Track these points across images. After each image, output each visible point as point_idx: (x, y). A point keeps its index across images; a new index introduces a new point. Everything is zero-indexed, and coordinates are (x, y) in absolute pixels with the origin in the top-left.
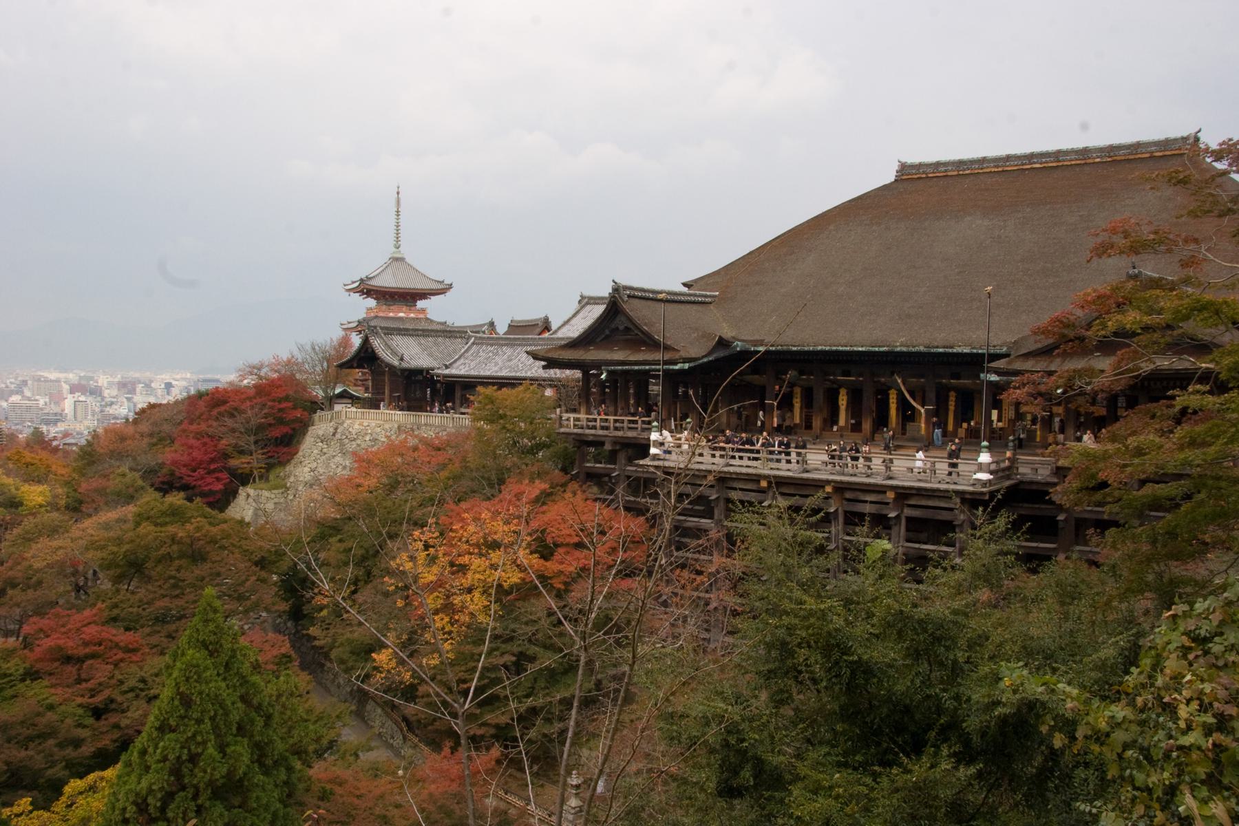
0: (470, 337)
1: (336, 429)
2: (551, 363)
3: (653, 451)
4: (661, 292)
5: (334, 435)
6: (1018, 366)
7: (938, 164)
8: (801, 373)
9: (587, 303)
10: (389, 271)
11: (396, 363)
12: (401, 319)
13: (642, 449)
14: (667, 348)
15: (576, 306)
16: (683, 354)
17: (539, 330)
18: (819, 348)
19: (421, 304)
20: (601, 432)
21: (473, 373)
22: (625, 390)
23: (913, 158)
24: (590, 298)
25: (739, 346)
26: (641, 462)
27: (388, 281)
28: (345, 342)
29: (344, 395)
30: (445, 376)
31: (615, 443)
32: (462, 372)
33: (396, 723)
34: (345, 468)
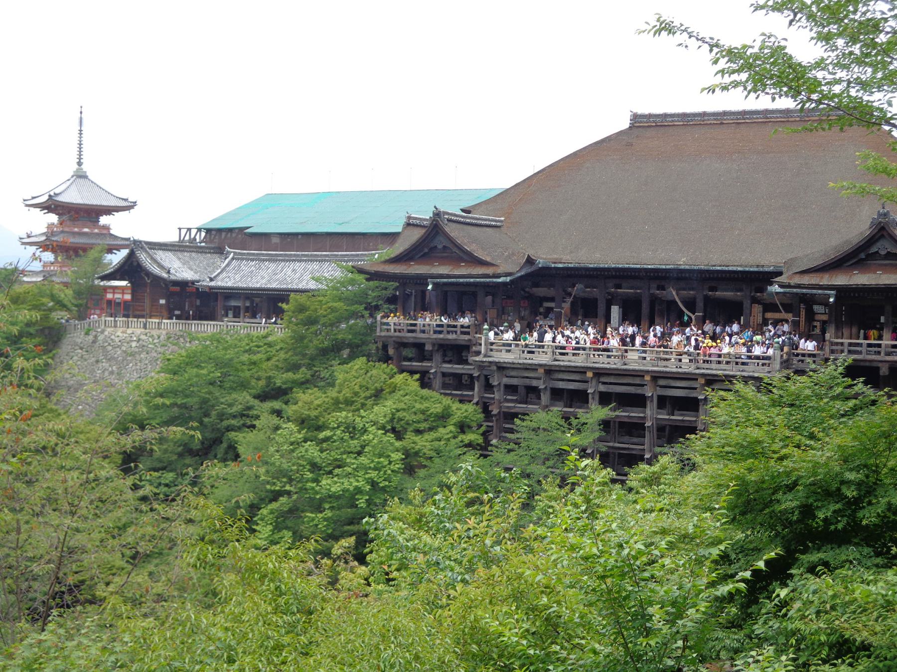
0: (229, 253)
1: (96, 337)
5: (94, 342)
6: (797, 280)
8: (586, 287)
10: (73, 187)
11: (165, 275)
12: (86, 234)
19: (104, 220)
21: (240, 285)
22: (458, 298)
25: (541, 263)
27: (73, 197)
30: (211, 288)
31: (433, 345)
32: (230, 284)
34: (112, 373)
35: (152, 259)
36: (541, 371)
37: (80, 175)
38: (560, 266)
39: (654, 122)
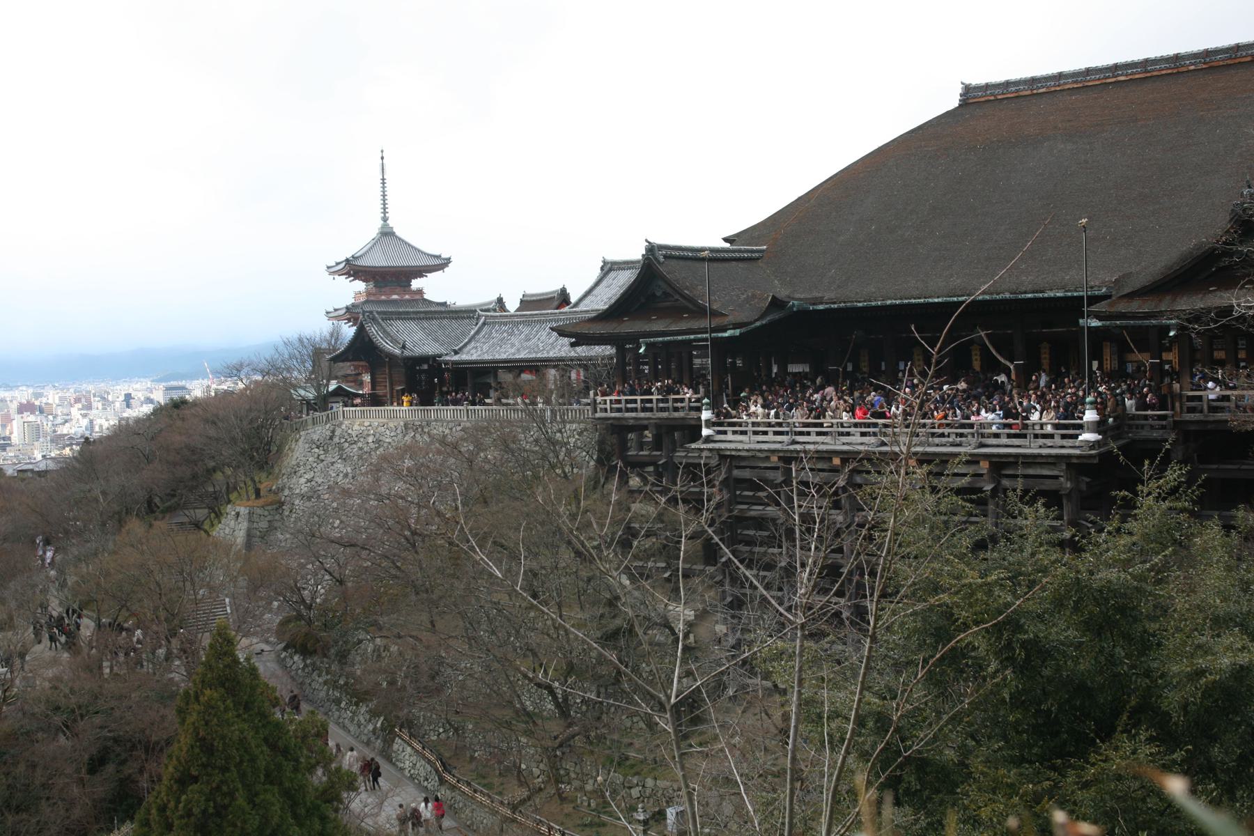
1: (333, 432)
2: (580, 339)
3: (705, 432)
4: (703, 250)
5: (331, 438)
6: (1122, 307)
7: (1008, 84)
9: (610, 270)
10: (378, 247)
11: (397, 351)
12: (395, 301)
13: (693, 431)
14: (714, 314)
15: (596, 273)
16: (731, 319)
17: (556, 303)
18: (889, 302)
19: (416, 284)
20: (642, 415)
21: (486, 357)
23: (979, 78)
24: (614, 263)
26: (693, 446)
27: (378, 260)
28: (335, 334)
29: (339, 392)
30: (454, 363)
32: (474, 357)
33: (429, 762)
34: (346, 475)
35: (385, 332)
36: (774, 459)
37: (387, 233)
38: (821, 307)
39: (992, 94)
